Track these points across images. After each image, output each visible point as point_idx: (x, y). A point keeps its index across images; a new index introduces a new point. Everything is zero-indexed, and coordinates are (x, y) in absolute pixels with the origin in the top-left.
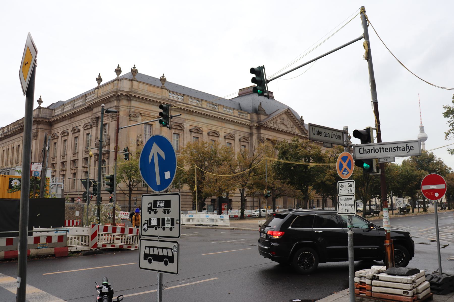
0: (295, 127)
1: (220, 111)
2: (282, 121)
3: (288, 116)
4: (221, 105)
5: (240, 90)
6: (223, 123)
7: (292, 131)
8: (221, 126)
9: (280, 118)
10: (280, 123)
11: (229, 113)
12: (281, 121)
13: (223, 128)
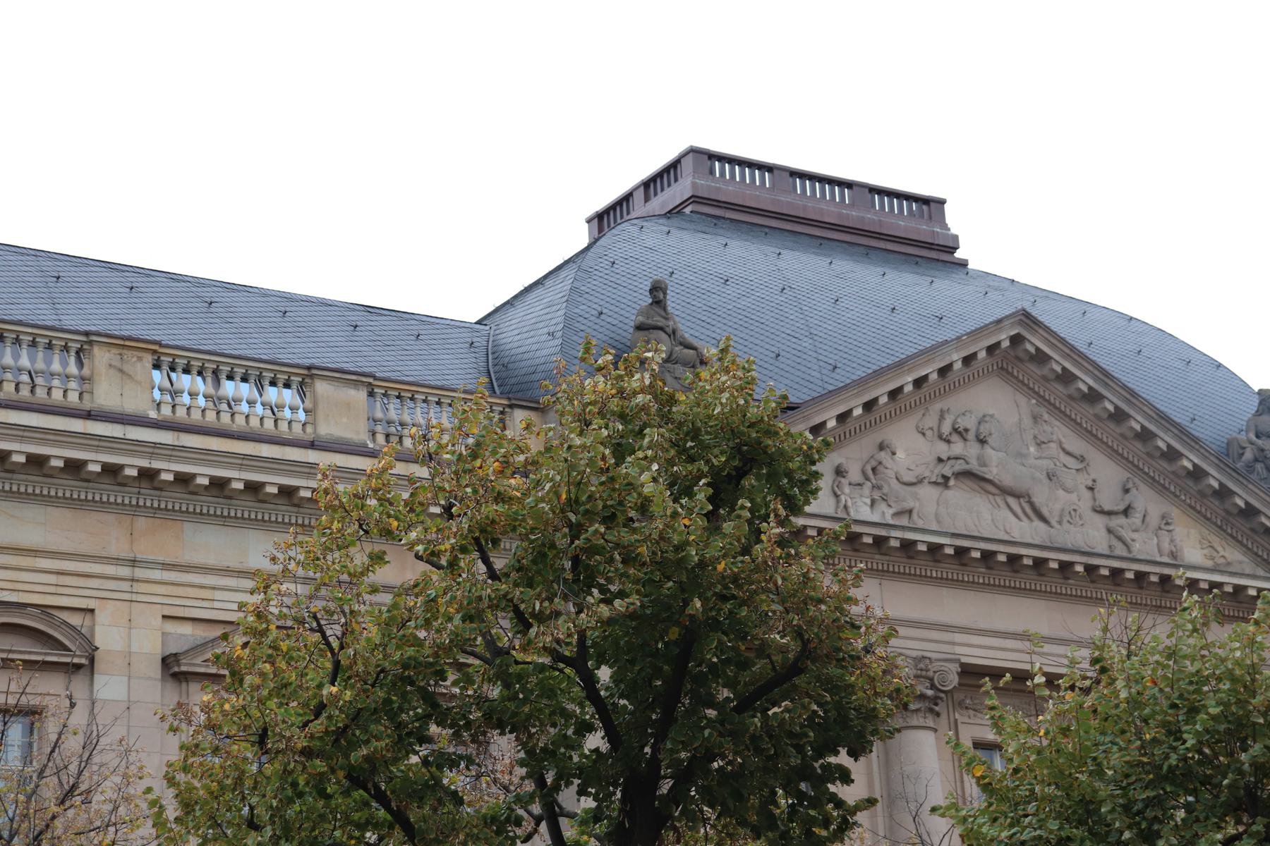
0: (1146, 501)
1: (107, 395)
2: (958, 448)
3: (1043, 400)
4: (124, 343)
5: (589, 221)
6: (141, 523)
7: (1120, 550)
8: (117, 544)
9: (931, 421)
10: (935, 472)
11: (134, 403)
12: (943, 450)
13: (140, 573)
